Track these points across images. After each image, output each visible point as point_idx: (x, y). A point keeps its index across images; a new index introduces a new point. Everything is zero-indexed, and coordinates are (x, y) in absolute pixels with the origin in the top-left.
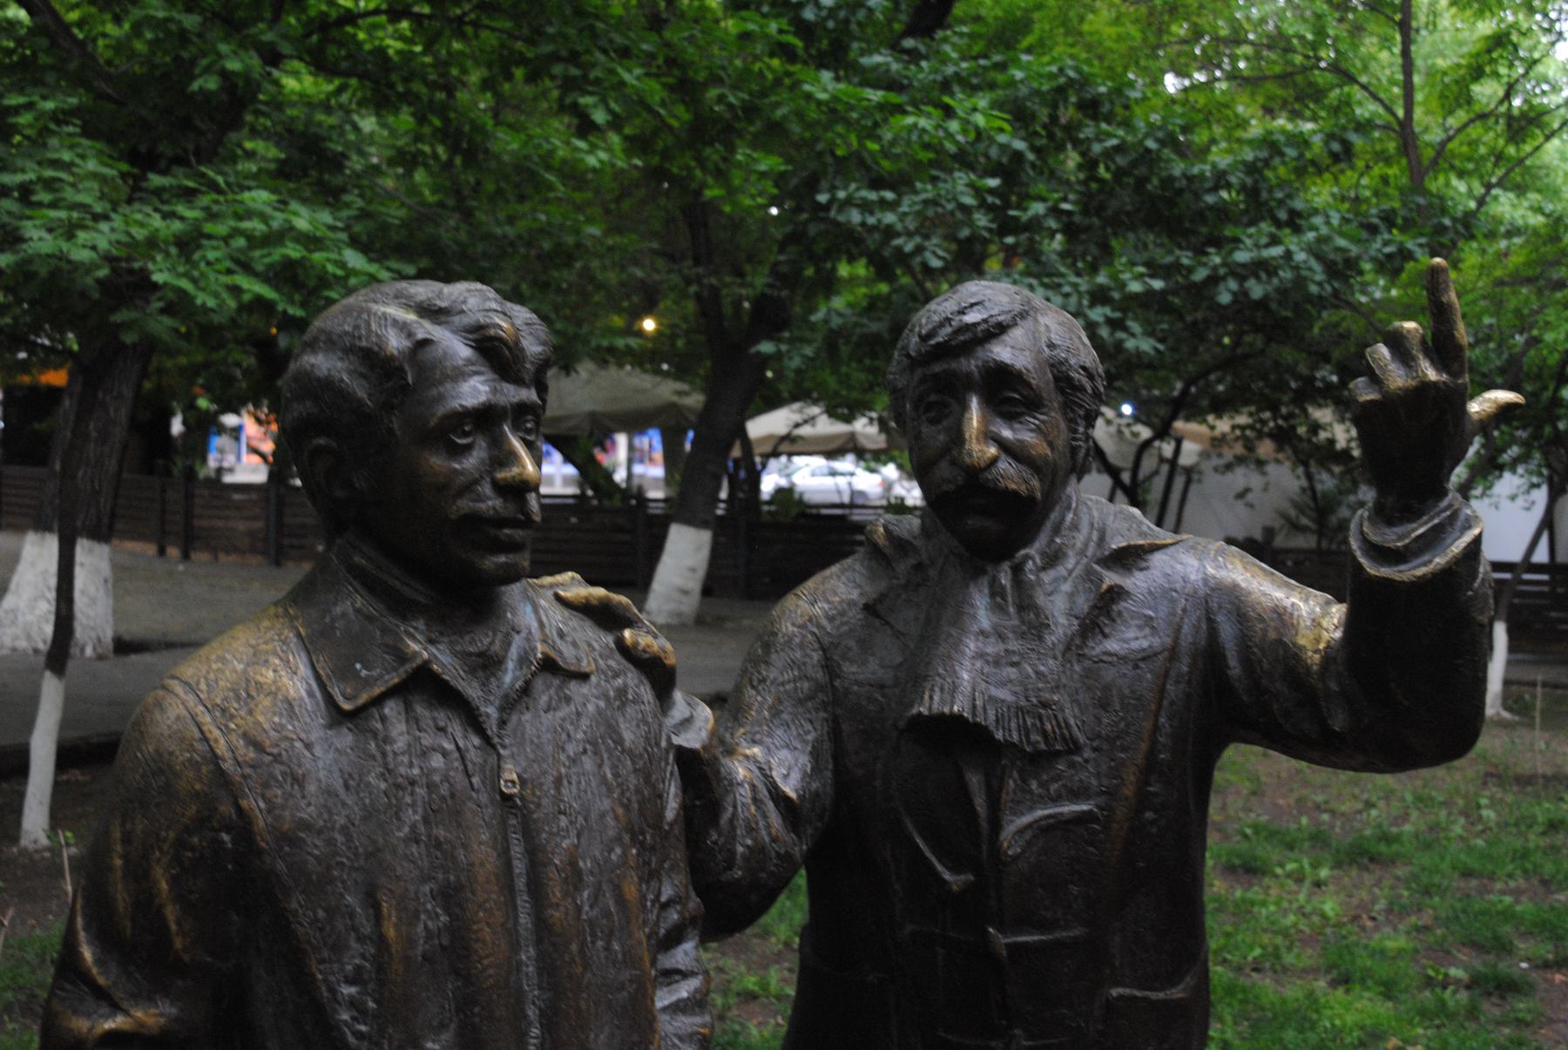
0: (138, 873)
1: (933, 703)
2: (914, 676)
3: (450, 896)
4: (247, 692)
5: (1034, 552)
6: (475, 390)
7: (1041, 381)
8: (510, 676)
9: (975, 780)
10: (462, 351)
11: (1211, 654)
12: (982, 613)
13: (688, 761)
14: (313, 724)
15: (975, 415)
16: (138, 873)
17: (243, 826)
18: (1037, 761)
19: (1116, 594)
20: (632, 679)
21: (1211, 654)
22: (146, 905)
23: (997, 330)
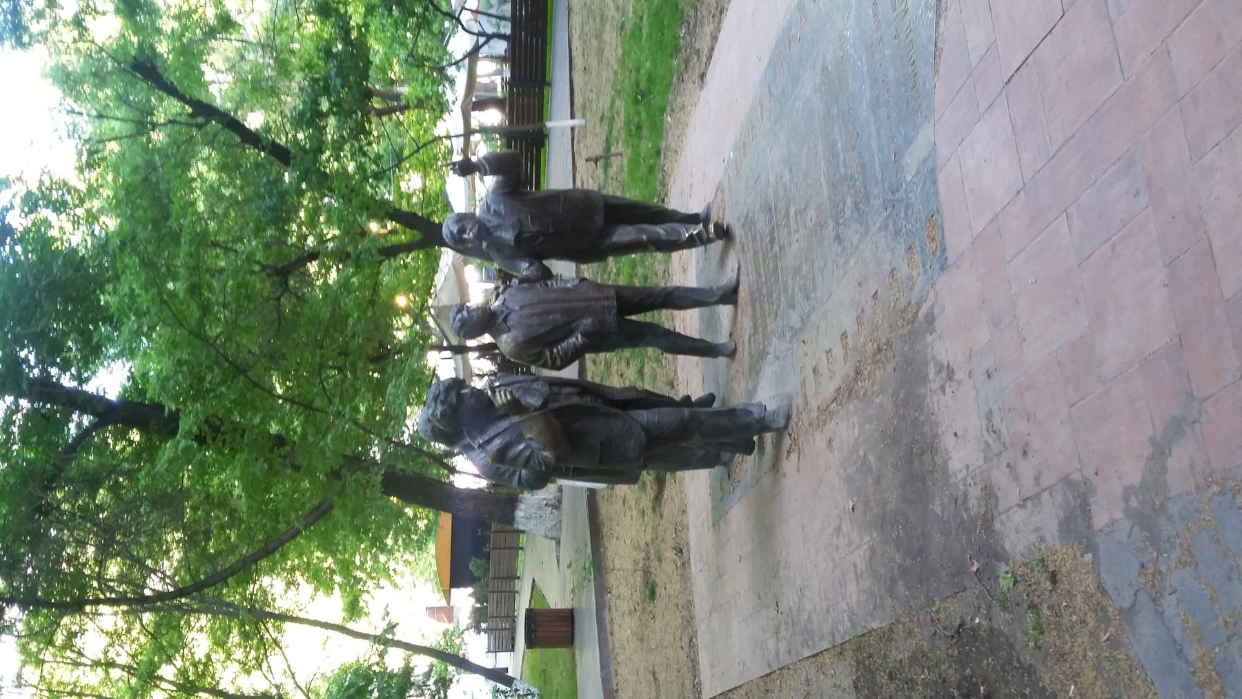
0: (529, 356)
1: (512, 243)
2: (510, 247)
3: (532, 315)
4: (506, 342)
5: (488, 225)
6: (465, 313)
7: (460, 225)
8: (504, 309)
9: (526, 235)
10: (459, 316)
11: (504, 194)
12: (498, 233)
13: (520, 283)
14: (510, 334)
15: (466, 236)
16: (529, 356)
17: (523, 342)
18: (520, 223)
19: (495, 211)
20: (508, 291)
21: (504, 194)
22: (534, 355)
23: (451, 232)
